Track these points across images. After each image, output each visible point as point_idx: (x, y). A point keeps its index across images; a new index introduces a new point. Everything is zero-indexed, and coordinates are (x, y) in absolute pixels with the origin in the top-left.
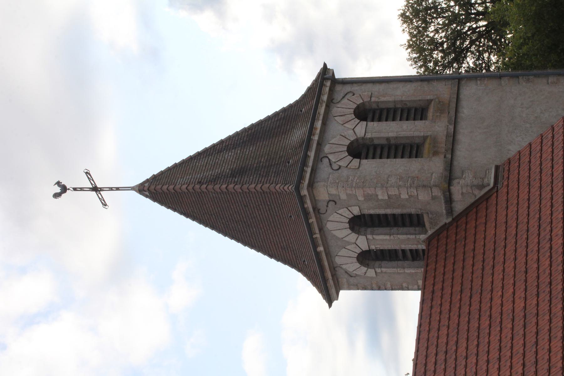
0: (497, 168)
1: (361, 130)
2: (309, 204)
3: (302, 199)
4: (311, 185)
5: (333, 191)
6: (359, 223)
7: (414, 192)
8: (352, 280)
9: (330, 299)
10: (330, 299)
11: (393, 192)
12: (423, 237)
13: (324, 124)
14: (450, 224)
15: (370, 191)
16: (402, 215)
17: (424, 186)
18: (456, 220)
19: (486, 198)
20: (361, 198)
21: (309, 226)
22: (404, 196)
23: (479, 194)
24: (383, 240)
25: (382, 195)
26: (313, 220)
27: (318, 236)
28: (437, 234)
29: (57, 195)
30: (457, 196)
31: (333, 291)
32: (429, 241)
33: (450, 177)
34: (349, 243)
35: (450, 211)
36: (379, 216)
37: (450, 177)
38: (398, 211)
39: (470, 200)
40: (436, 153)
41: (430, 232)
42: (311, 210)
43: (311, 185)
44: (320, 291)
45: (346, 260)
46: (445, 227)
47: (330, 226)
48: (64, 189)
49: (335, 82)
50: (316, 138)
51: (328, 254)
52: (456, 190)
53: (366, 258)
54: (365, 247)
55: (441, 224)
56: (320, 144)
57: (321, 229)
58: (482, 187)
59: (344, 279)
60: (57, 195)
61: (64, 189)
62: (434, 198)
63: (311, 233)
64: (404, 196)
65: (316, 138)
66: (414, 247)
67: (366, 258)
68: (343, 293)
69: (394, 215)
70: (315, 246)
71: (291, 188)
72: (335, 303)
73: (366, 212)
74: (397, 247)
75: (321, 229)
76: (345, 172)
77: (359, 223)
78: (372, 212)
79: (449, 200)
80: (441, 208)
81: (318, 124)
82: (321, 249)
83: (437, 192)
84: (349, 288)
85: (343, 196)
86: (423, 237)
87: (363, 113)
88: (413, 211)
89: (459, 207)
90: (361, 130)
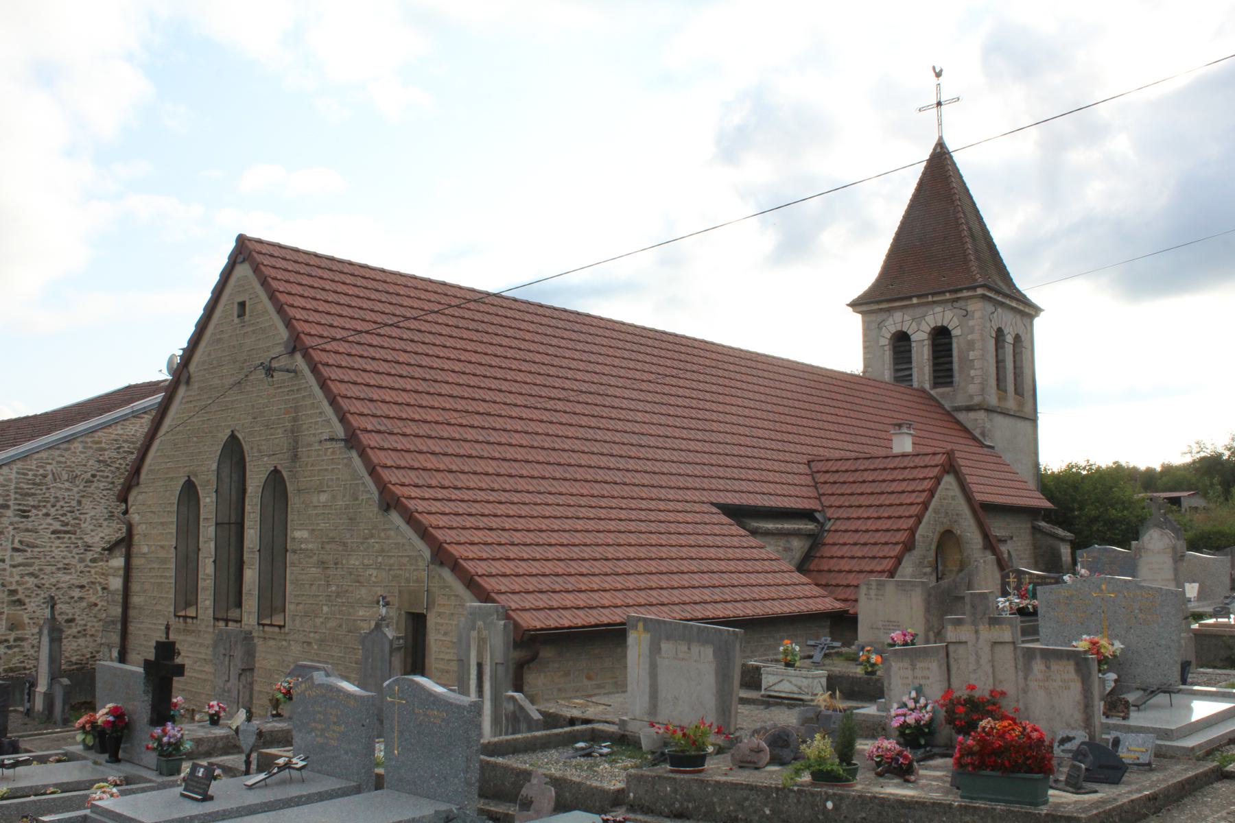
0: (992, 447)
1: (1010, 339)
2: (965, 294)
3: (974, 288)
4: (984, 297)
5: (977, 315)
6: (941, 336)
7: (977, 381)
8: (874, 325)
9: (855, 305)
10: (855, 305)
11: (977, 364)
12: (927, 386)
13: (1013, 309)
14: (944, 409)
15: (978, 345)
16: (951, 370)
17: (983, 389)
18: (948, 414)
19: (975, 439)
20: (969, 337)
21: (943, 293)
22: (972, 373)
23: (977, 433)
24: (922, 354)
25: (972, 355)
26: (948, 296)
27: (930, 299)
28: (932, 398)
29: (934, 68)
30: (972, 415)
31: (864, 308)
32: (924, 391)
33: (989, 410)
34: (919, 324)
35: (958, 409)
36: (951, 350)
37: (989, 410)
38: (956, 366)
39: (969, 426)
40: (1000, 399)
41: (932, 392)
42: (959, 295)
43: (984, 297)
44: (860, 297)
45: (896, 321)
46: (941, 406)
47: (938, 309)
48: (938, 75)
49: (1031, 317)
50: (1007, 302)
51: (906, 306)
52: (981, 415)
53: (901, 341)
54: (913, 338)
55: (943, 402)
56: (1002, 304)
57: (934, 302)
58: (983, 434)
59: (873, 317)
60: (934, 68)
61: (938, 75)
62: (971, 397)
63: (933, 294)
64: (972, 373)
65: (1007, 302)
66: (915, 377)
67: (901, 341)
68: (859, 316)
69: (951, 363)
70: (918, 296)
71: (980, 281)
72: (850, 309)
73: (954, 341)
74: (914, 364)
75: (934, 302)
76: (988, 325)
77: (941, 336)
78: (955, 346)
79: (969, 409)
80: (961, 401)
81: (1014, 304)
82: (915, 301)
83: (977, 400)
84: (864, 322)
85: (971, 323)
86: (927, 386)
87: (1017, 338)
88: (957, 377)
89: (962, 416)
90: (1010, 339)
